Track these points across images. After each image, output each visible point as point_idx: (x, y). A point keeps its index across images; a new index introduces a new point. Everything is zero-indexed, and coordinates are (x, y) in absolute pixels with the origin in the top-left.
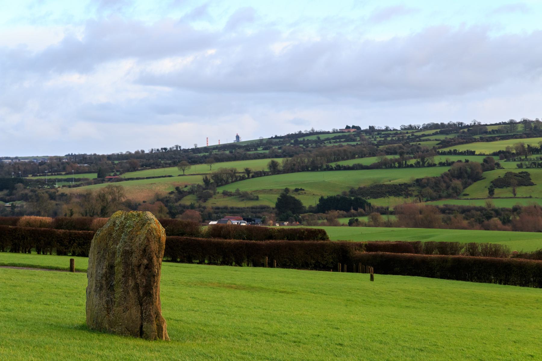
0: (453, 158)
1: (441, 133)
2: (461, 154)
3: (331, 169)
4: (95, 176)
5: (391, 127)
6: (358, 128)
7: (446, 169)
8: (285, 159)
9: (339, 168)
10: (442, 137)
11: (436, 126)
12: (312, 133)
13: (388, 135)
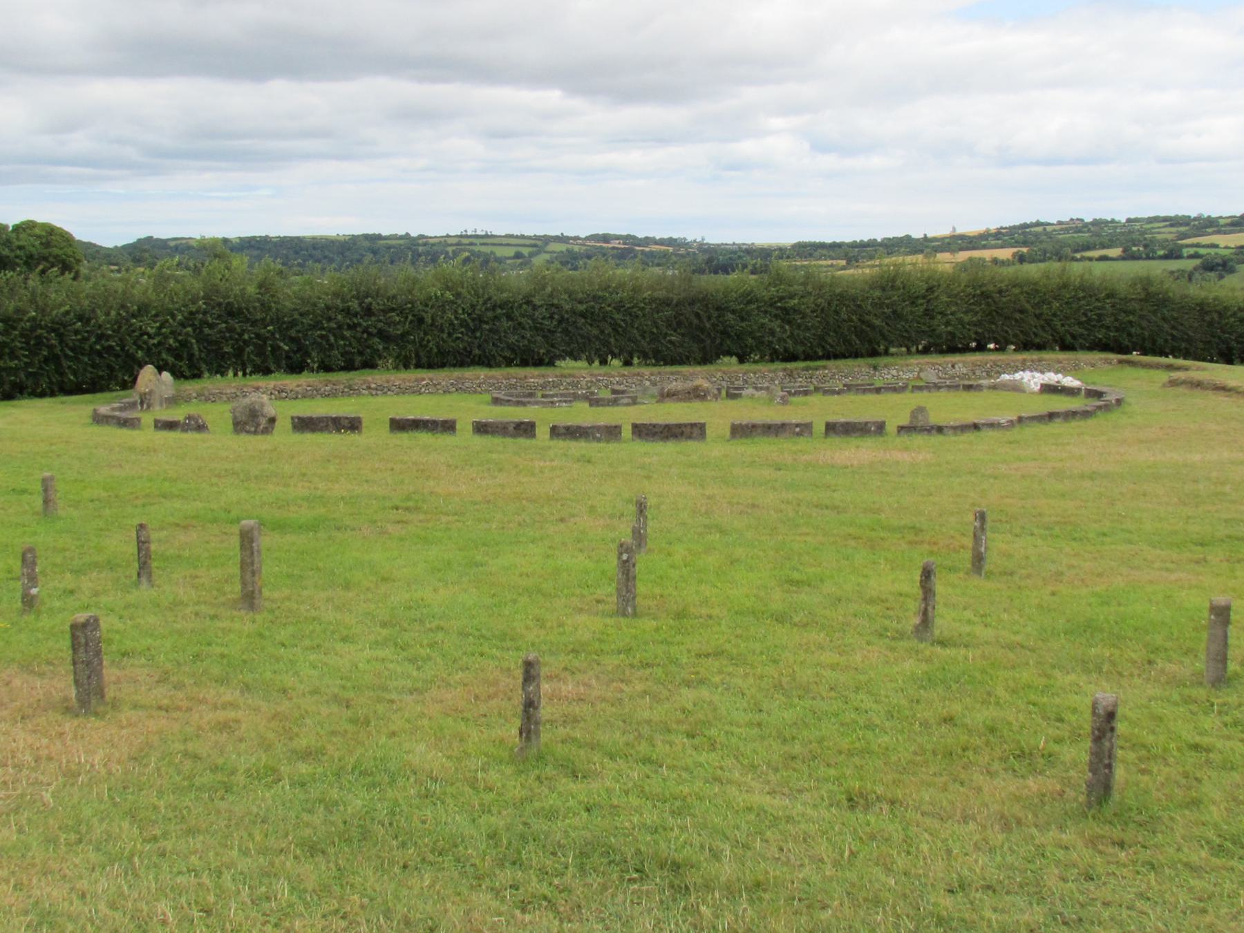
0: (1202, 251)
1: (1172, 226)
2: (1204, 246)
3: (1077, 260)
4: (843, 262)
5: (1117, 219)
6: (1082, 220)
7: (1197, 262)
8: (1015, 250)
9: (1083, 259)
10: (1174, 229)
11: (1165, 219)
12: (1038, 224)
13: (1116, 227)
